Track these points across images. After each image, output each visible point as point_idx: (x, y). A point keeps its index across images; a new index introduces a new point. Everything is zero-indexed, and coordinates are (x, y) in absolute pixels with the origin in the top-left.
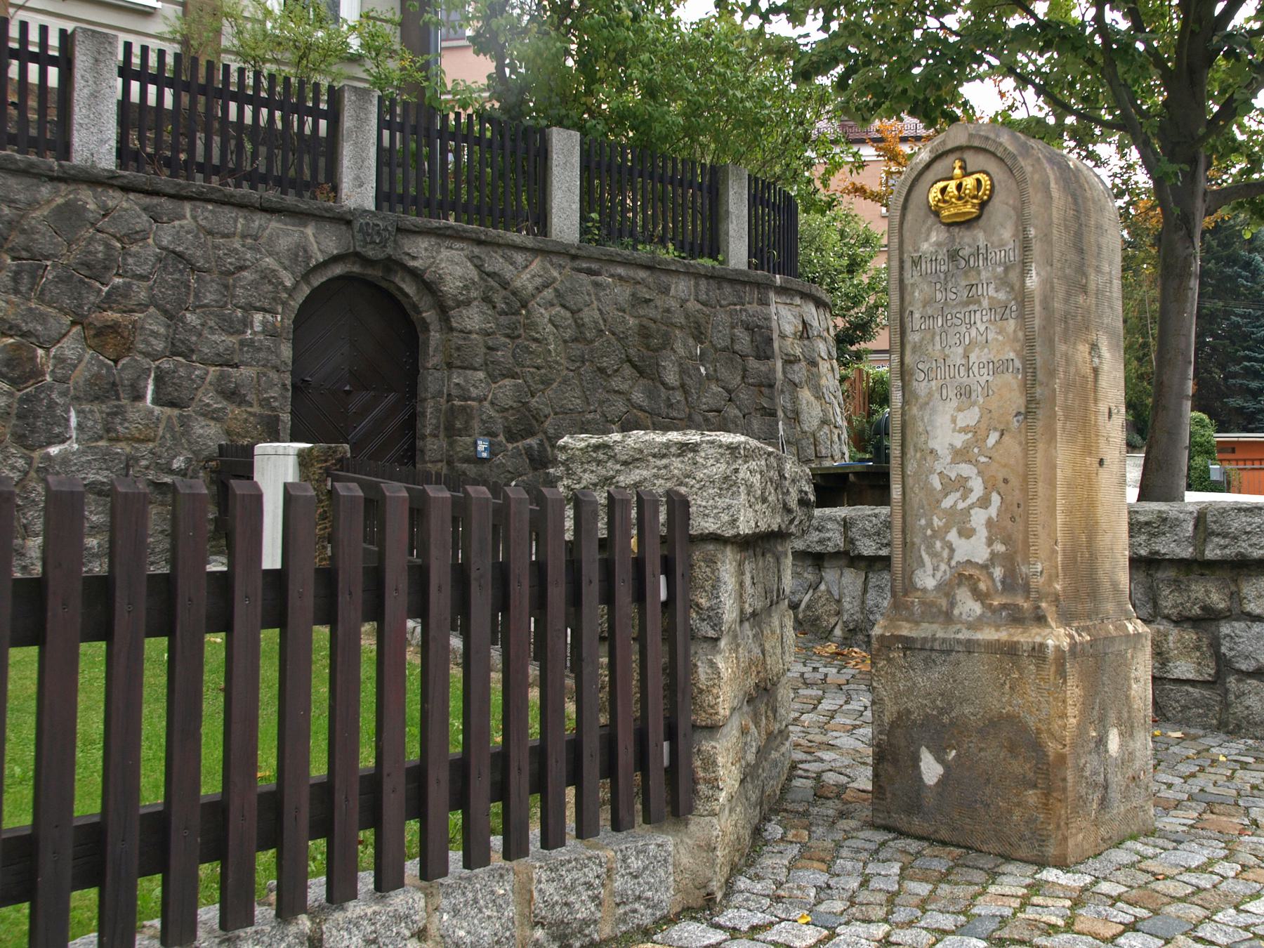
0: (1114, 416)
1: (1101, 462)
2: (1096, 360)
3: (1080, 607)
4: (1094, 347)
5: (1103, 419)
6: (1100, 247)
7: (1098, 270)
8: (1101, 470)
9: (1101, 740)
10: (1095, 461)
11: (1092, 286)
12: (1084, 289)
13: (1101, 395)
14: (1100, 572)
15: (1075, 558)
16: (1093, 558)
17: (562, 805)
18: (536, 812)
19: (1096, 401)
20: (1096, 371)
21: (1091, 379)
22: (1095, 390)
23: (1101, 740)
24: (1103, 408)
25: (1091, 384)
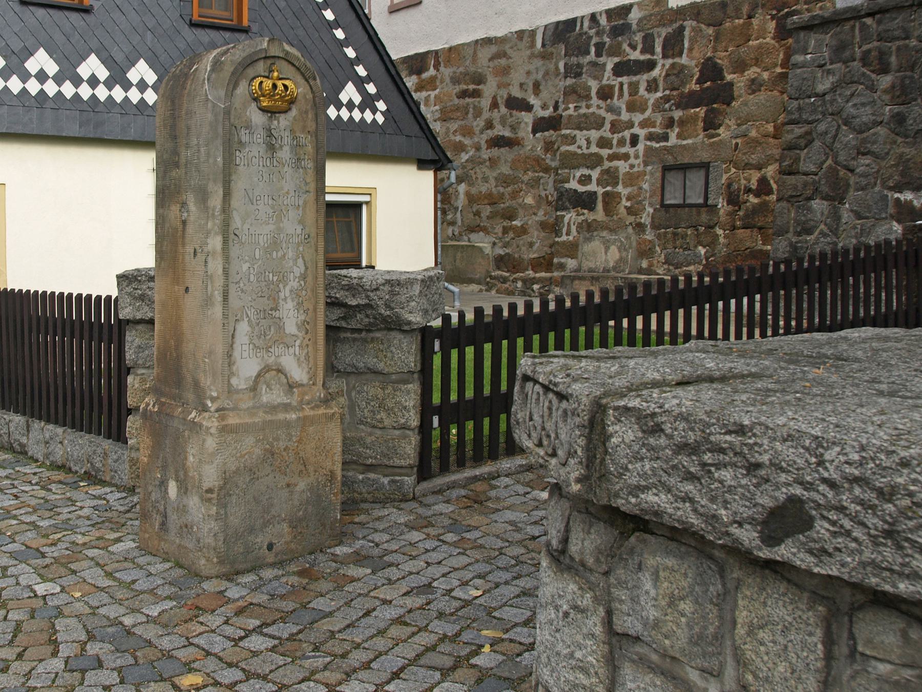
0: (199, 254)
1: (187, 290)
2: (185, 214)
3: (167, 389)
4: (184, 204)
5: (189, 258)
6: (189, 128)
7: (188, 146)
8: (186, 295)
9: (163, 482)
10: (183, 288)
11: (183, 161)
12: (177, 165)
13: (187, 240)
14: (185, 370)
15: (166, 355)
16: (179, 357)
17: (892, 275)
18: (883, 275)
19: (184, 245)
20: (184, 223)
21: (180, 228)
22: (183, 237)
23: (163, 482)
24: (189, 249)
25: (180, 233)
